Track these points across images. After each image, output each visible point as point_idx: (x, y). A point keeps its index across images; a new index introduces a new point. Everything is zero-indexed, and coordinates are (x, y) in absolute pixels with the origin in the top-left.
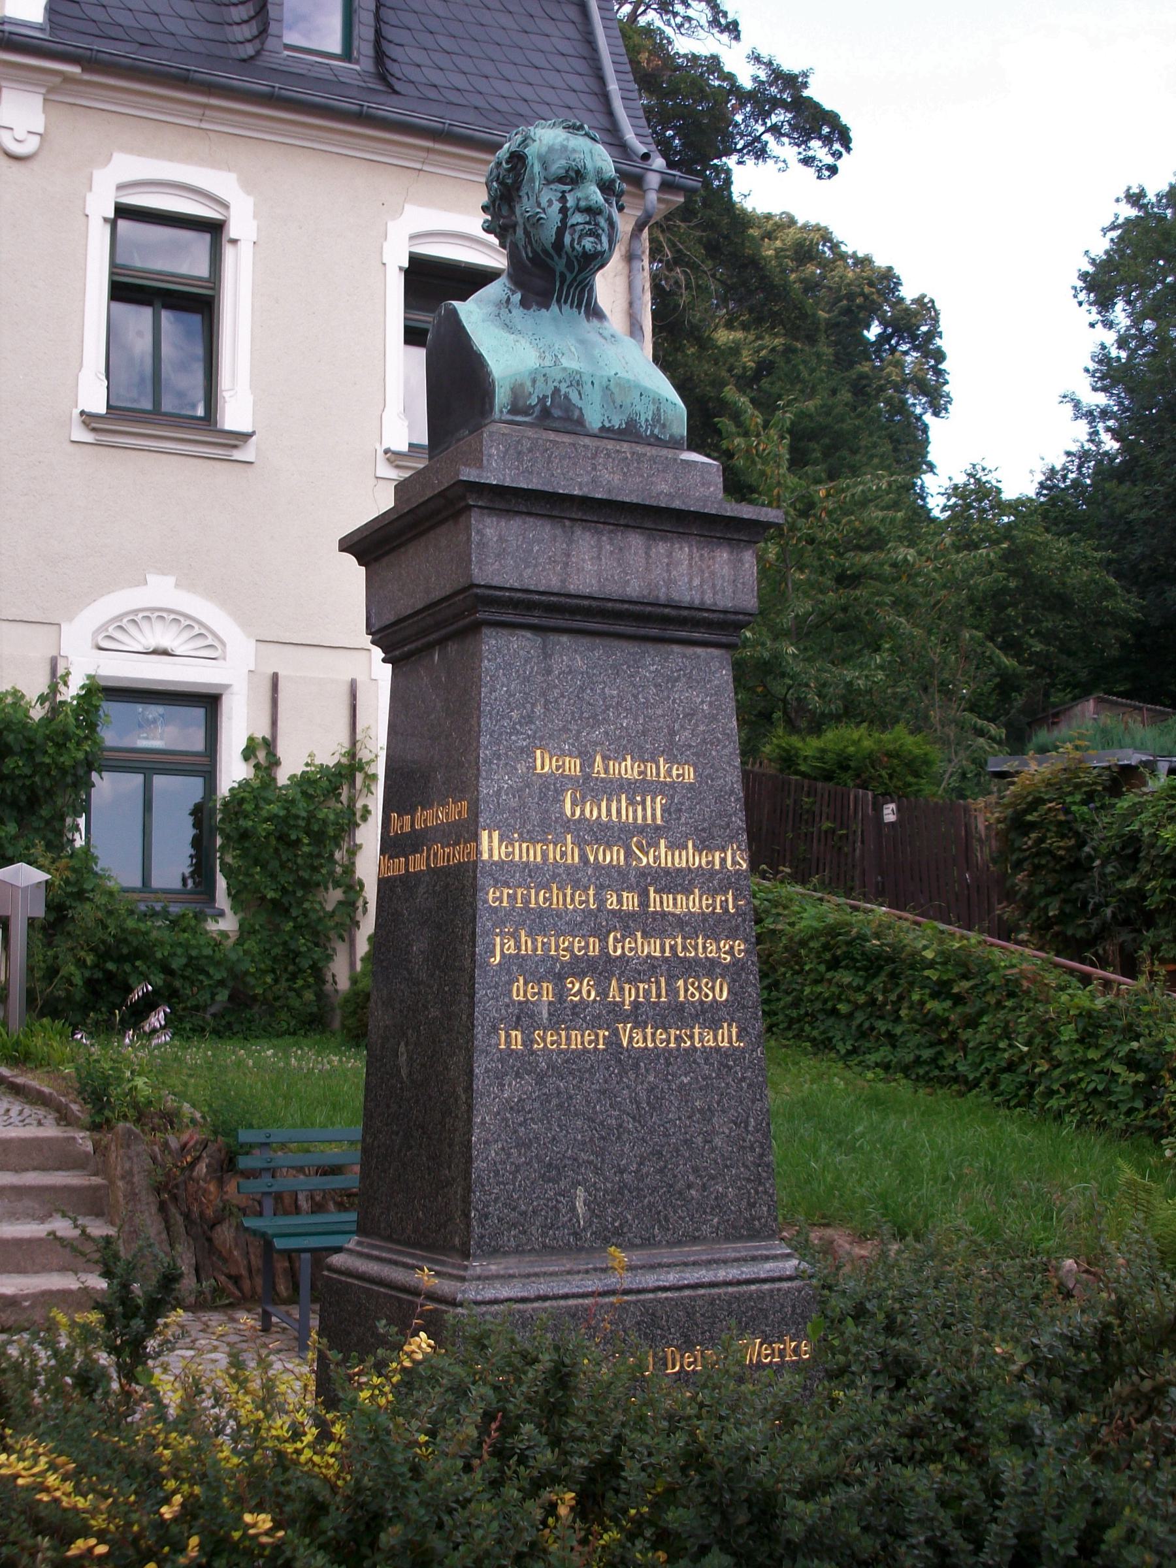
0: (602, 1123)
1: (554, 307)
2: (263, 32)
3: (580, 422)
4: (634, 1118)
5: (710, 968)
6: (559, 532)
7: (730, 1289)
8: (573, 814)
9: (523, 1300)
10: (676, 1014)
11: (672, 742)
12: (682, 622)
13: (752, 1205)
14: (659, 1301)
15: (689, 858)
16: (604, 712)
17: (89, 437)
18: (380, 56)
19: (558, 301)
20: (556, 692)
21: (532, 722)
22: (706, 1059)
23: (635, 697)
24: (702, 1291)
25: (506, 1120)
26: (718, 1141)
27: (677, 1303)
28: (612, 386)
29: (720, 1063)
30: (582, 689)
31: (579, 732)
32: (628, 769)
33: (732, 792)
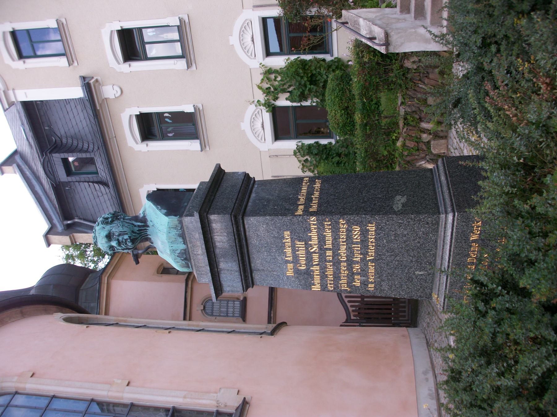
3: (185, 250)
5: (349, 231)
6: (222, 272)
7: (453, 241)
10: (364, 242)
11: (277, 237)
12: (239, 235)
13: (428, 223)
15: (314, 235)
20: (269, 268)
22: (379, 234)
23: (265, 247)
24: (452, 249)
25: (394, 290)
26: (405, 233)
27: (454, 257)
29: (380, 230)
32: (289, 251)
33: (290, 220)
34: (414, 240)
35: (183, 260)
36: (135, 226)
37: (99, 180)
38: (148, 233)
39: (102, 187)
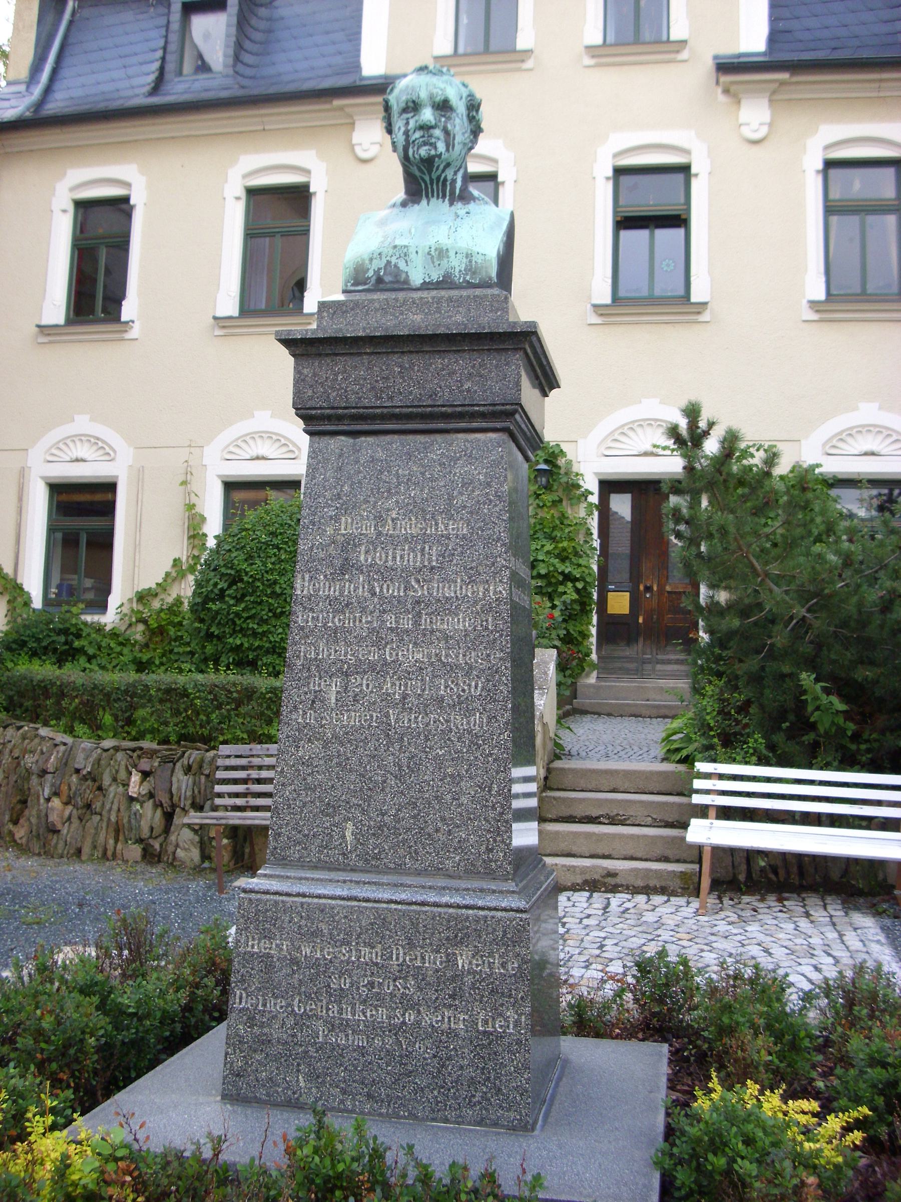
0: (370, 778)
1: (424, 202)
3: (406, 281)
4: (396, 777)
7: (451, 910)
8: (366, 561)
9: (288, 895)
11: (450, 505)
12: (461, 416)
13: (489, 850)
14: (390, 910)
16: (397, 487)
19: (427, 196)
20: (361, 476)
21: (340, 498)
22: (459, 738)
23: (423, 474)
24: (427, 908)
26: (464, 800)
27: (404, 914)
28: (433, 253)
30: (381, 472)
31: (376, 502)
33: (499, 539)
34: (443, 819)
35: (377, 272)
36: (455, 173)
37: (168, 76)
38: (433, 201)
39: (152, 78)
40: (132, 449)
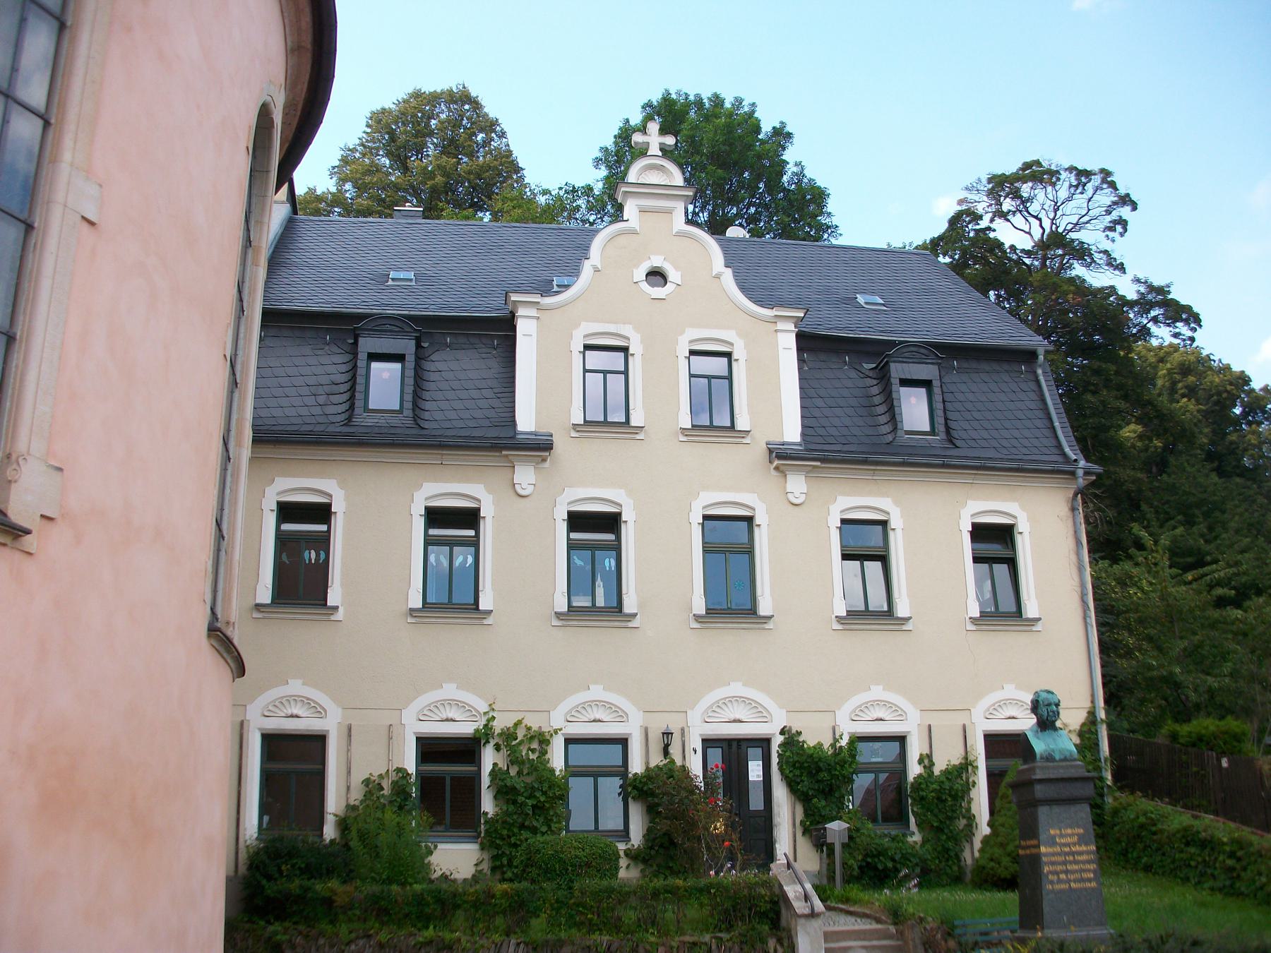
2: (895, 429)
5: (1089, 871)
10: (1082, 880)
15: (1084, 848)
17: (840, 627)
18: (948, 429)
32: (1069, 831)
40: (340, 710)
